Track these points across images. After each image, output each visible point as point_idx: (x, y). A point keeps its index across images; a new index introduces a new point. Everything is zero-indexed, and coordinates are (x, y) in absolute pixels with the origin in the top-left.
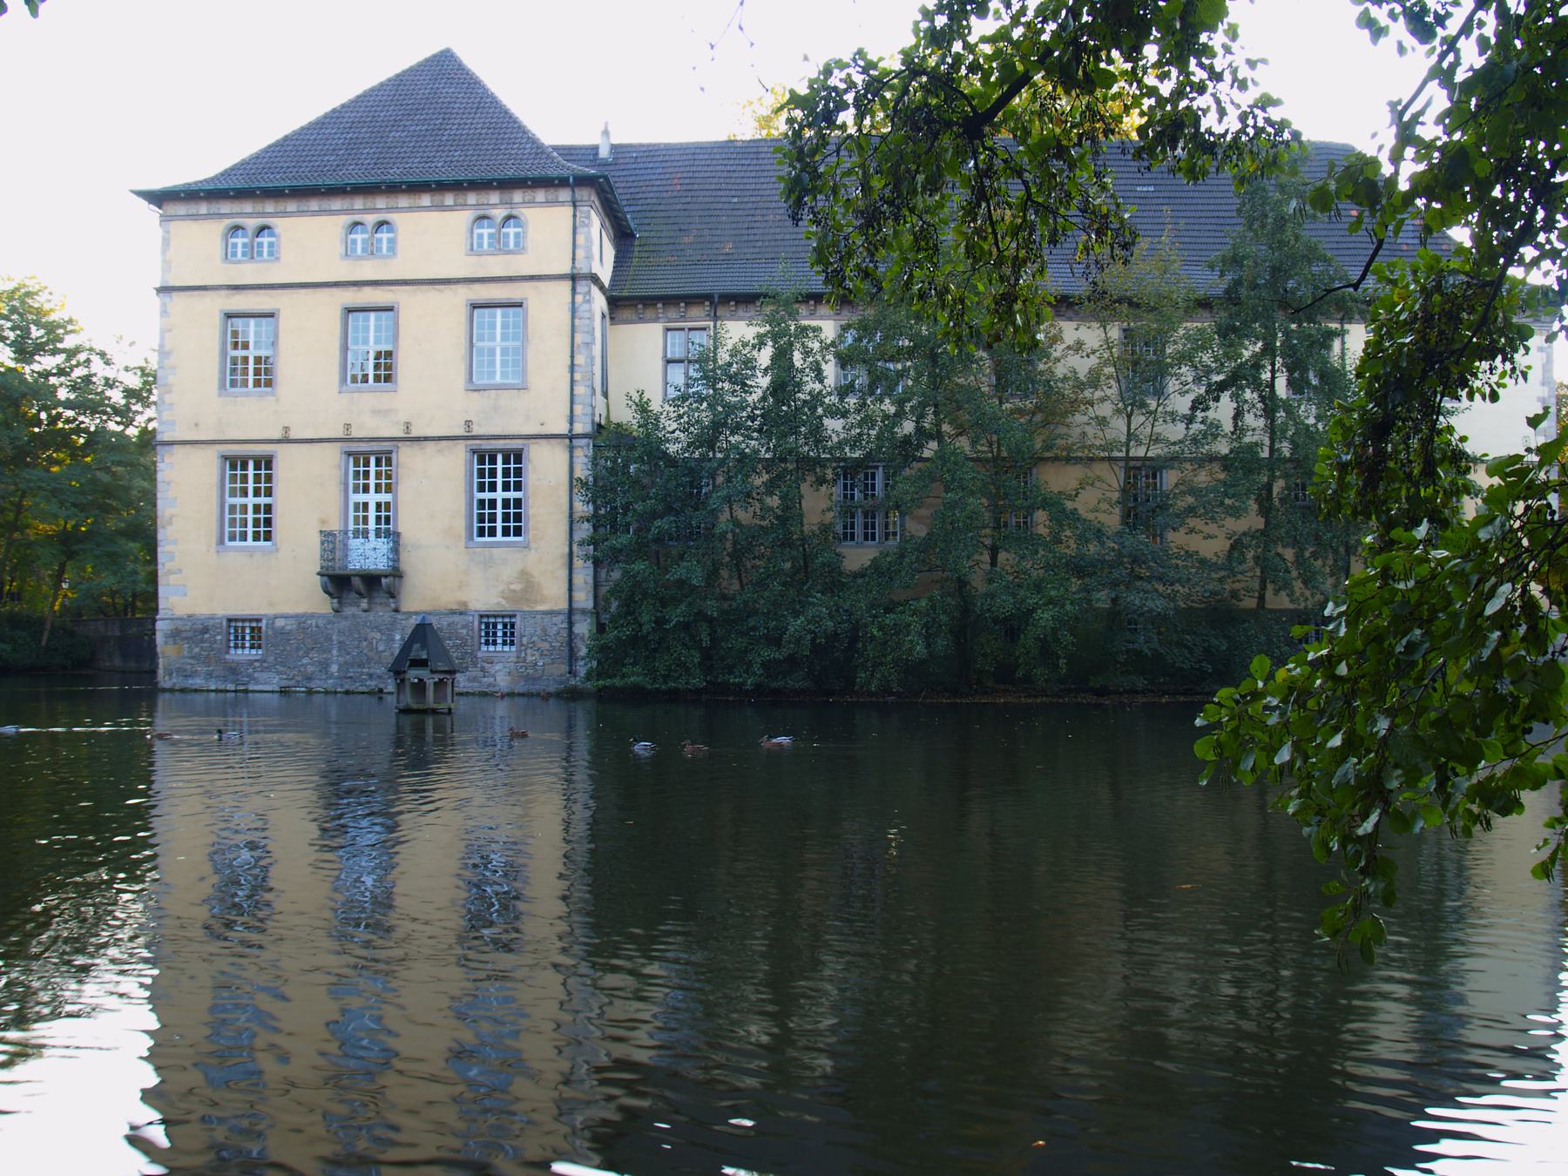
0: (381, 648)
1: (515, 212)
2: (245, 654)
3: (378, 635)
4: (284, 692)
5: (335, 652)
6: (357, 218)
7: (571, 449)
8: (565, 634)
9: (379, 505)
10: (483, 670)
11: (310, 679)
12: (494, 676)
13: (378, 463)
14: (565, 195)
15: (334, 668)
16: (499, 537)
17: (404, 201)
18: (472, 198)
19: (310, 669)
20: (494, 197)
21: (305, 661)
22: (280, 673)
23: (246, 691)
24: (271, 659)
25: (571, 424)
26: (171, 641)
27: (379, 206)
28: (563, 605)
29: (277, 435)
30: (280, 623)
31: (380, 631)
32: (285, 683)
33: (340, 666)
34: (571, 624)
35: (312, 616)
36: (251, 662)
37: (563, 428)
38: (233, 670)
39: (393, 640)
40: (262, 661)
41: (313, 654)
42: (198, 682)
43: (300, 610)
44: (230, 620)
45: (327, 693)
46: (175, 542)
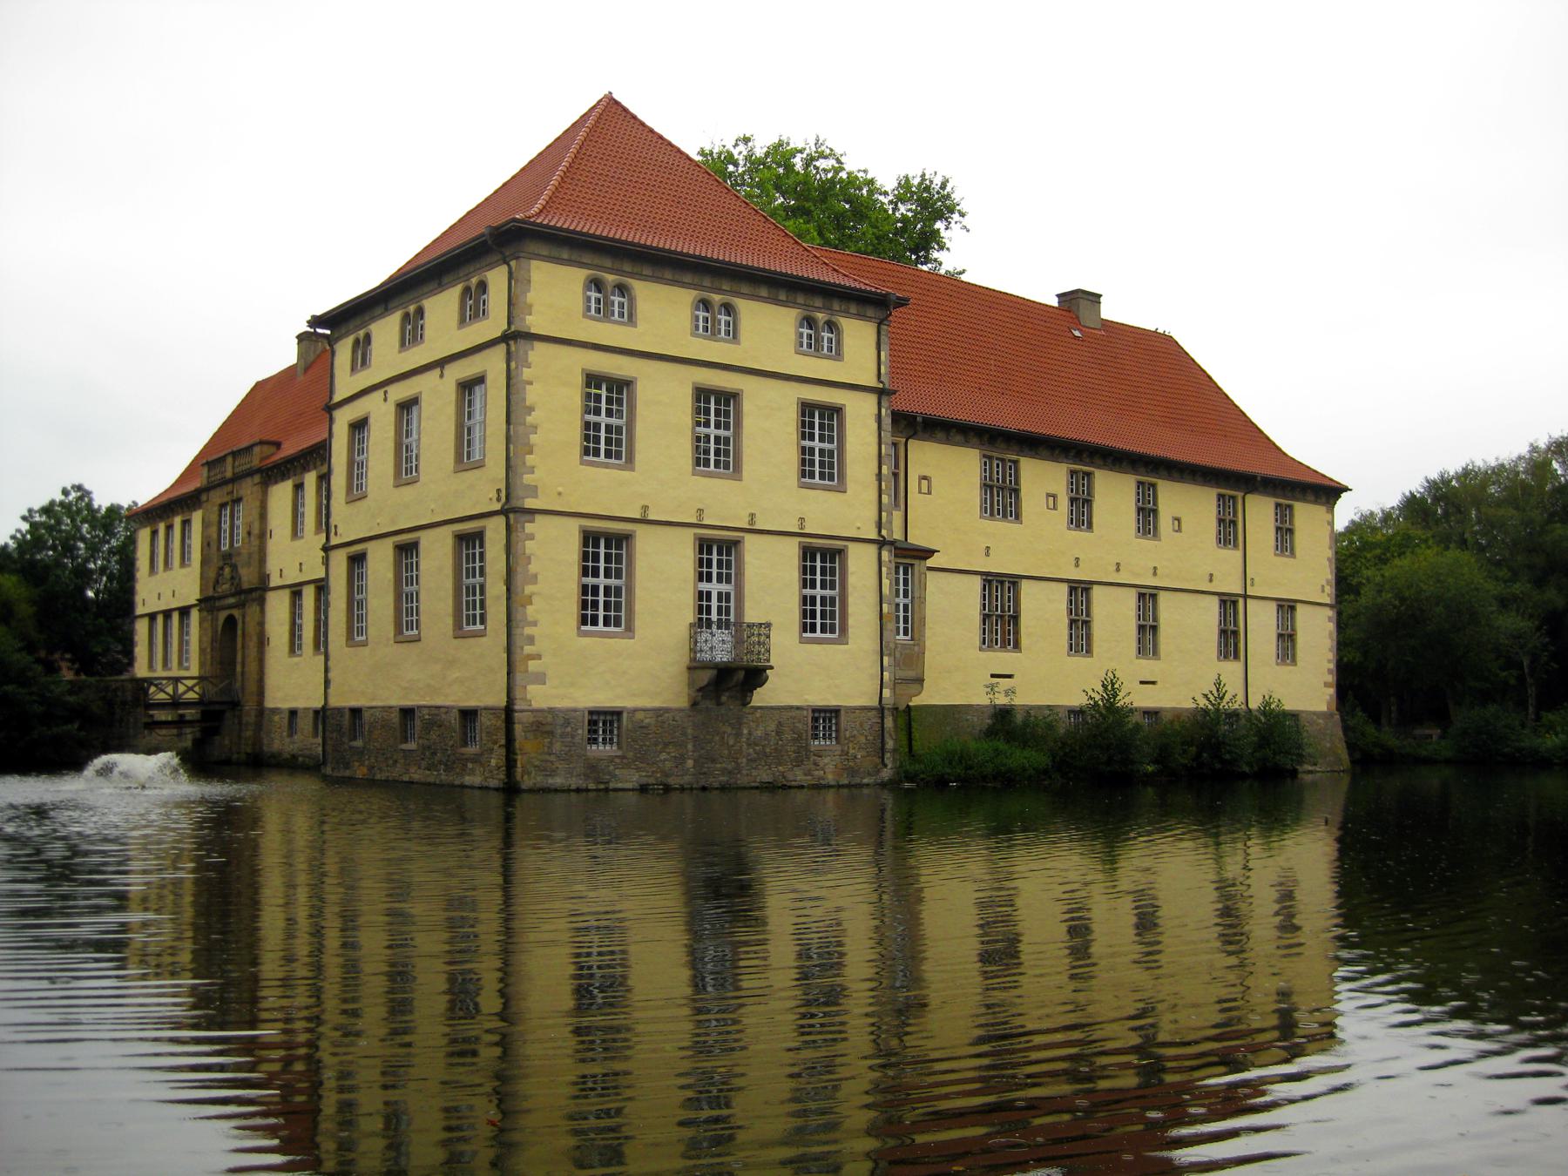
0: (731, 742)
1: (834, 319)
2: (601, 750)
3: (729, 730)
4: (643, 789)
5: (690, 747)
6: (705, 295)
7: (880, 550)
8: (877, 728)
9: (720, 594)
10: (816, 764)
11: (667, 775)
12: (823, 769)
13: (720, 553)
14: (870, 312)
15: (690, 763)
16: (818, 634)
17: (745, 289)
18: (800, 299)
19: (668, 764)
20: (818, 302)
21: (663, 756)
22: (638, 769)
23: (607, 790)
24: (630, 755)
25: (880, 531)
26: (531, 736)
27: (724, 287)
28: (875, 703)
29: (638, 516)
30: (640, 716)
31: (730, 724)
32: (644, 781)
33: (695, 761)
34: (882, 718)
35: (667, 710)
36: (611, 759)
37: (873, 535)
38: (593, 768)
39: (742, 734)
40: (623, 757)
41: (671, 748)
42: (558, 781)
43: (657, 704)
44: (591, 713)
45: (682, 789)
46: (535, 624)
